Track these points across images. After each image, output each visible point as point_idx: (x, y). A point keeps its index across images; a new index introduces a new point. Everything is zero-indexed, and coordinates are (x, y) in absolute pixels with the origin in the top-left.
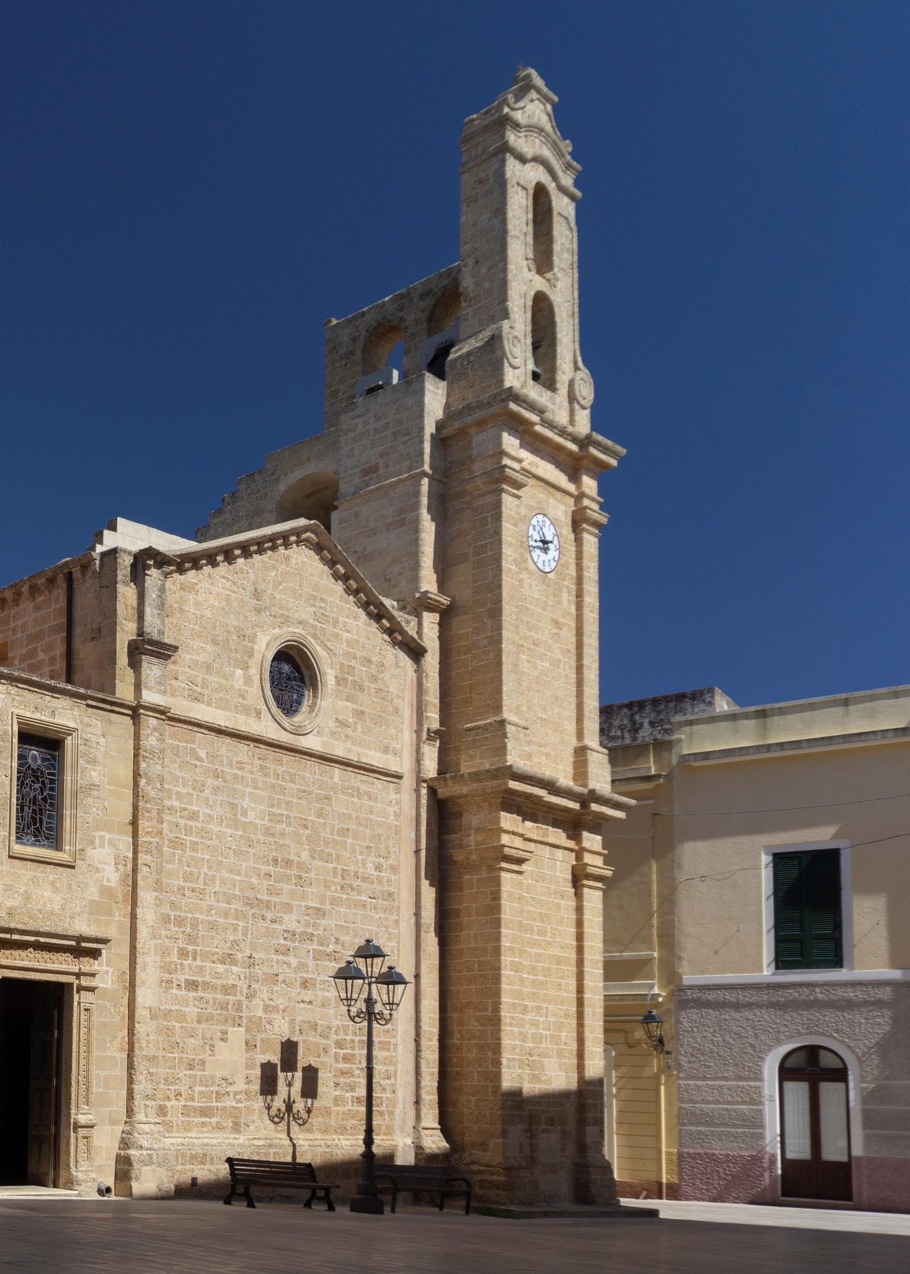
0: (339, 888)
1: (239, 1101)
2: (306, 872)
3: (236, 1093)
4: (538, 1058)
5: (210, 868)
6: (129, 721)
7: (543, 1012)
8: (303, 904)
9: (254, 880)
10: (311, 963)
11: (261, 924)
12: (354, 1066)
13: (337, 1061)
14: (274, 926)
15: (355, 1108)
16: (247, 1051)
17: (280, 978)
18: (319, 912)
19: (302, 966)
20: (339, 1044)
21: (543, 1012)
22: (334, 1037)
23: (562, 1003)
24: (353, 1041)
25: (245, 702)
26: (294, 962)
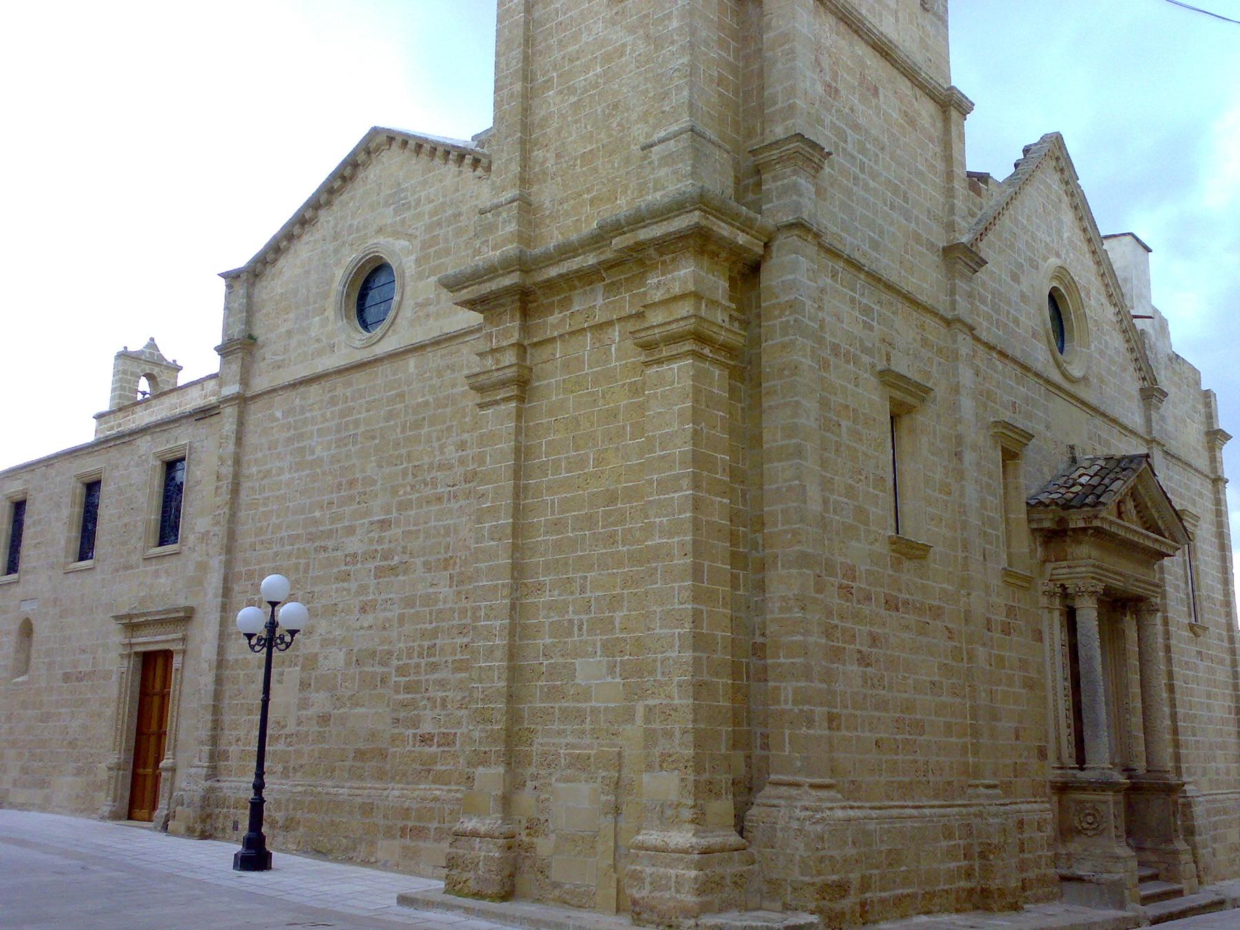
0: (409, 488)
1: (290, 744)
2: (371, 485)
3: (287, 736)
4: (561, 660)
5: (278, 517)
6: (253, 407)
7: (576, 586)
8: (366, 521)
9: (317, 514)
10: (372, 582)
11: (323, 555)
12: (418, 696)
13: (397, 692)
14: (336, 553)
15: (417, 749)
16: (301, 691)
17: (340, 606)
18: (384, 524)
19: (363, 589)
20: (401, 671)
21: (576, 586)
22: (395, 662)
23: (620, 564)
24: (418, 666)
25: (876, 167)
26: (353, 586)
